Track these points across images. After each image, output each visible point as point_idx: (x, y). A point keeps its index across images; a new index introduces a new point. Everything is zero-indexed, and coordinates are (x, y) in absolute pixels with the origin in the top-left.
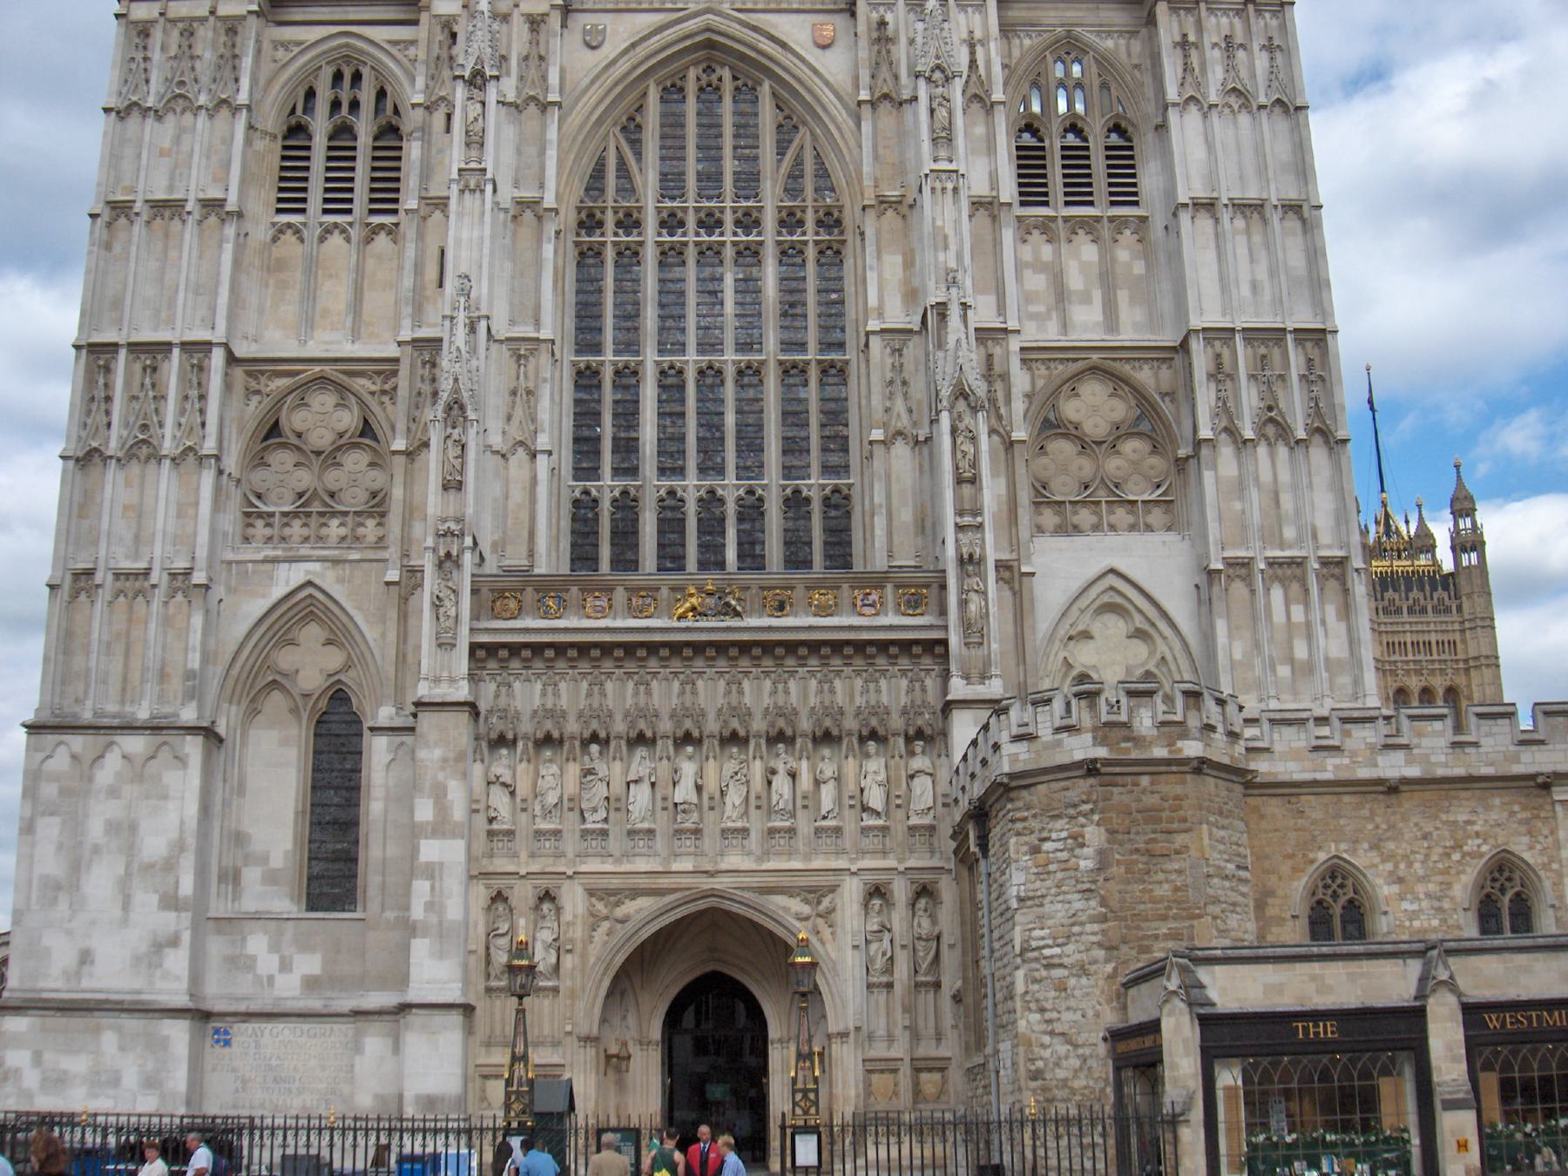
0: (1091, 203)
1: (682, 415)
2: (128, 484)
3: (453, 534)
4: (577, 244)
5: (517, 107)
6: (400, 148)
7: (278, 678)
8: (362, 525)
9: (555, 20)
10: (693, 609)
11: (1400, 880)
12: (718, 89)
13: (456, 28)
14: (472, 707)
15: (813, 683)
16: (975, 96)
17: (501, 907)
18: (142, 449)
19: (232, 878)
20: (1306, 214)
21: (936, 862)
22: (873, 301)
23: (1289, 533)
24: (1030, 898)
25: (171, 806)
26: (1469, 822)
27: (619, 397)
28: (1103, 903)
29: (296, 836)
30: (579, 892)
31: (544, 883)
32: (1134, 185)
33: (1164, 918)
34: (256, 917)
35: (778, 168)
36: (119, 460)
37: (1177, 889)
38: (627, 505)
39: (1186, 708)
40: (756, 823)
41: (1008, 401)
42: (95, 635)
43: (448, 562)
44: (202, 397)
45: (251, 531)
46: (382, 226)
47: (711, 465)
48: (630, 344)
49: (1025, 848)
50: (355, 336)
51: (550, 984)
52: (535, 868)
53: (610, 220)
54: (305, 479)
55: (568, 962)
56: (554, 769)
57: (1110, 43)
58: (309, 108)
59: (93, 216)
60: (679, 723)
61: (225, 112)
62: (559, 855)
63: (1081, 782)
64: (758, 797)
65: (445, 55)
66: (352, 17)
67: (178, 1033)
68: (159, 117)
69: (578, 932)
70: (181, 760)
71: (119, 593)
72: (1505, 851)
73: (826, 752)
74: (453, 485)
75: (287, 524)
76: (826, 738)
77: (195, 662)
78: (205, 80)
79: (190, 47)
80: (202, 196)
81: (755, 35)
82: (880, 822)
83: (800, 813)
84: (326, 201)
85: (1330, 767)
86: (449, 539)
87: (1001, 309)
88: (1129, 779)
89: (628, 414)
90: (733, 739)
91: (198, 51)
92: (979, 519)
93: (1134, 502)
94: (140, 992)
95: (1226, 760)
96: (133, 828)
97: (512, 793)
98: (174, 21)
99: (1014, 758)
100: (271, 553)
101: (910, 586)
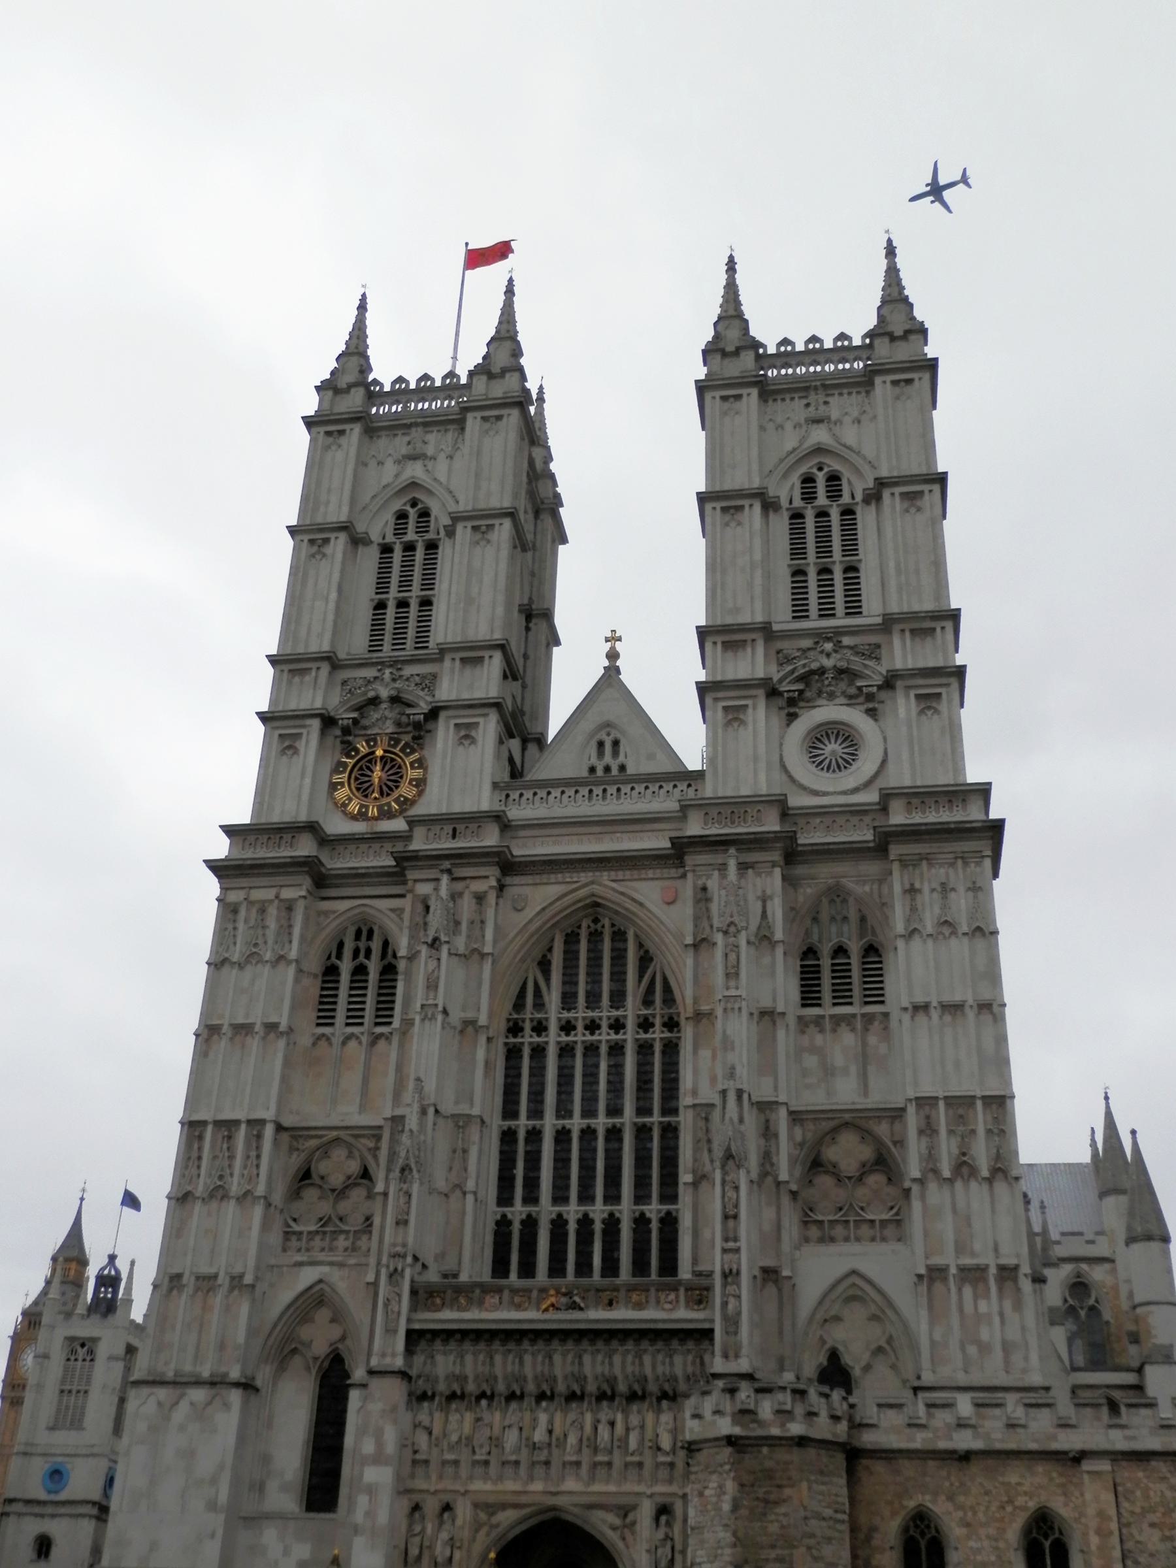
0: (851, 1004)
1: (569, 1160)
3: (399, 1256)
4: (506, 1044)
5: (465, 956)
7: (299, 1346)
8: (359, 1239)
9: (492, 898)
10: (553, 1305)
11: (968, 1525)
12: (602, 933)
14: (404, 1375)
15: (630, 1358)
16: (765, 936)
17: (417, 1515)
18: (218, 1193)
19: (259, 1488)
23: (977, 1247)
24: (698, 1528)
26: (1019, 1484)
27: (529, 1148)
28: (735, 1534)
30: (468, 1503)
31: (446, 1498)
32: (882, 989)
33: (773, 1547)
34: (268, 1517)
35: (639, 986)
36: (203, 1199)
37: (783, 1527)
38: (530, 1224)
39: (794, 1401)
40: (586, 1458)
41: (778, 1153)
43: (394, 1275)
44: (258, 1157)
45: (289, 1243)
46: (382, 1035)
47: (586, 1197)
48: (536, 1112)
49: (696, 1493)
50: (362, 1108)
52: (440, 1487)
53: (527, 1026)
54: (325, 1208)
55: (457, 1555)
56: (457, 1416)
57: (867, 888)
58: (339, 956)
59: (197, 1035)
60: (538, 1386)
62: (456, 1477)
64: (588, 1439)
65: (421, 923)
68: (241, 966)
69: (466, 1534)
70: (227, 1406)
71: (197, 1289)
72: (1045, 1507)
73: (635, 1407)
74: (402, 1222)
75: (312, 1239)
76: (633, 1397)
77: (241, 1338)
78: (270, 942)
79: (262, 920)
80: (266, 1021)
81: (622, 897)
82: (668, 1459)
83: (616, 1452)
84: (348, 1017)
85: (918, 1440)
86: (397, 1259)
87: (776, 1088)
88: (755, 1449)
89: (533, 1161)
90: (572, 1397)
91: (268, 924)
92: (738, 1244)
93: (872, 1221)
95: (829, 1437)
97: (430, 1433)
100: (299, 1258)
101: (696, 1289)
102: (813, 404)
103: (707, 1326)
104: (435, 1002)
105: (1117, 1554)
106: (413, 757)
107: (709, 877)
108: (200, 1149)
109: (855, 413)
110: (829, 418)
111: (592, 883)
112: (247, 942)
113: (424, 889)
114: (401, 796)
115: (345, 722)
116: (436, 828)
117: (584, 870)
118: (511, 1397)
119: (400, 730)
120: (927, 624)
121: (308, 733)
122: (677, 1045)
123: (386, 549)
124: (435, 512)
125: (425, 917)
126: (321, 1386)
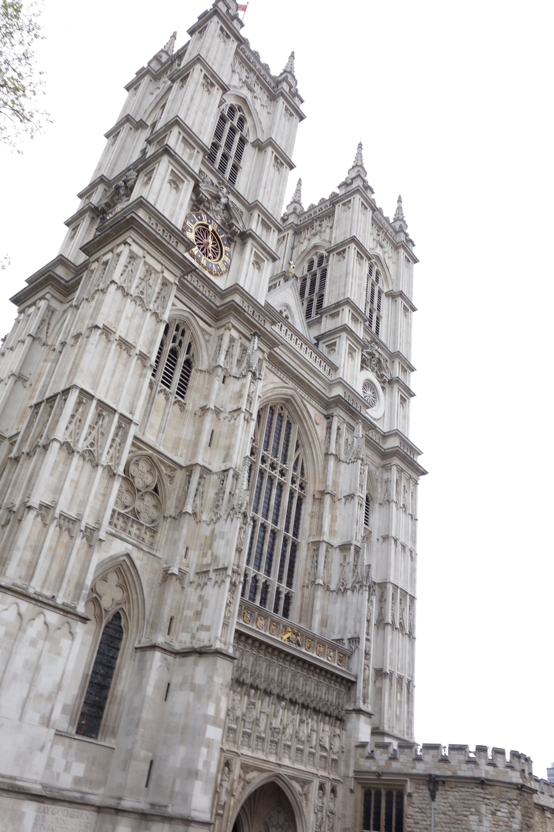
2: (76, 469)
6: (190, 372)
10: (289, 638)
20: (413, 555)
21: (337, 777)
25: (61, 661)
29: (82, 687)
31: (228, 755)
42: (47, 545)
49: (489, 812)
56: (239, 698)
61: (154, 318)
62: (235, 742)
63: (514, 791)
64: (297, 732)
73: (315, 717)
74: (239, 551)
77: (89, 582)
78: (154, 299)
83: (306, 743)
91: (151, 282)
94: (15, 779)
96: (37, 668)
98: (145, 263)
99: (487, 772)
102: (380, 237)
103: (353, 679)
104: (251, 411)
107: (341, 424)
108: (85, 414)
109: (391, 255)
110: (384, 247)
111: (295, 390)
112: (137, 287)
115: (204, 197)
117: (291, 379)
119: (222, 227)
120: (405, 367)
121: (188, 185)
122: (301, 499)
123: (223, 119)
124: (248, 125)
126: (104, 633)
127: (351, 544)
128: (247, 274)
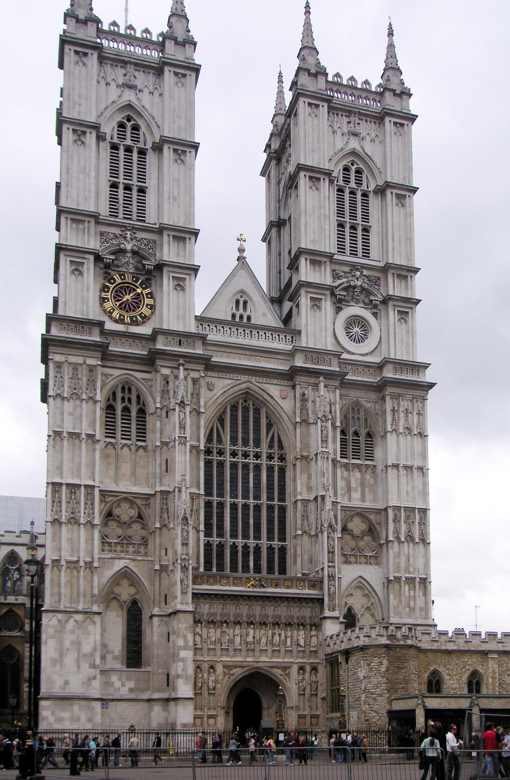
10: (252, 585)
11: (450, 675)
13: (168, 380)
22: (299, 489)
26: (468, 661)
31: (211, 663)
34: (113, 670)
51: (213, 692)
52: (209, 659)
55: (219, 686)
56: (213, 630)
62: (215, 655)
66: (128, 367)
67: (97, 705)
85: (435, 646)
87: (335, 494)
97: (201, 637)
105: (497, 684)
106: (148, 291)
113: (166, 371)
114: (142, 313)
116: (170, 338)
118: (239, 623)
119: (138, 272)
125: (167, 387)
127: (317, 496)
128: (169, 304)
